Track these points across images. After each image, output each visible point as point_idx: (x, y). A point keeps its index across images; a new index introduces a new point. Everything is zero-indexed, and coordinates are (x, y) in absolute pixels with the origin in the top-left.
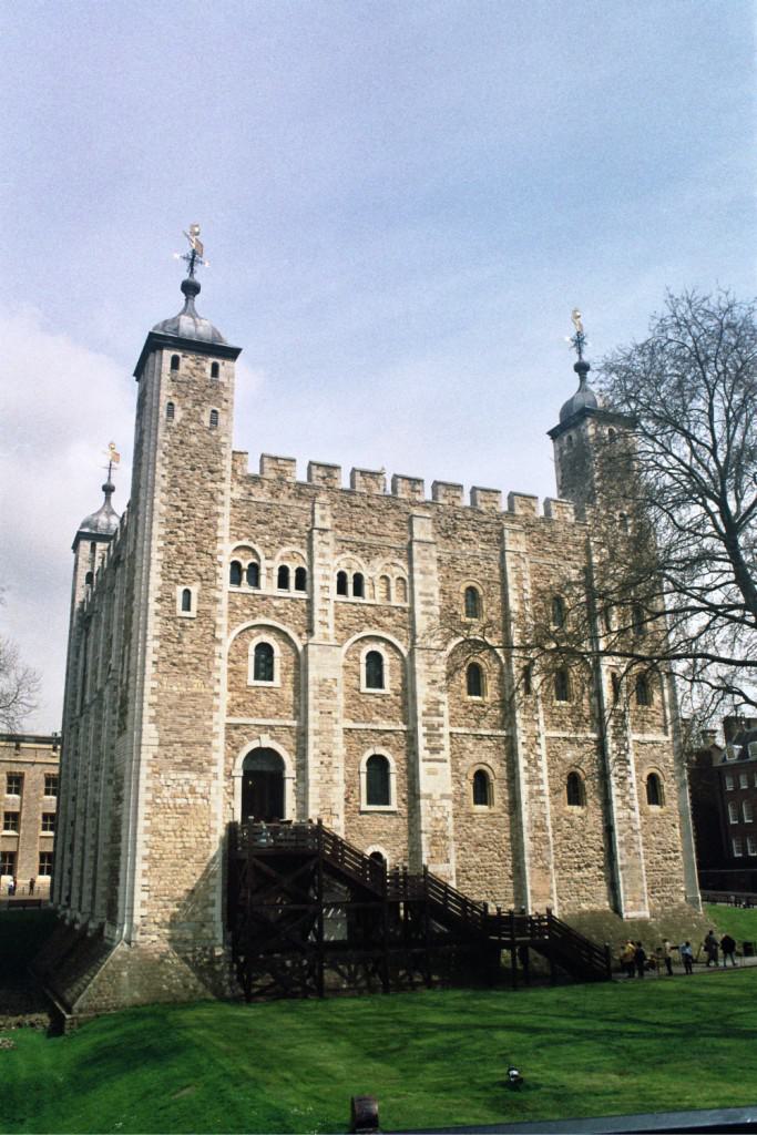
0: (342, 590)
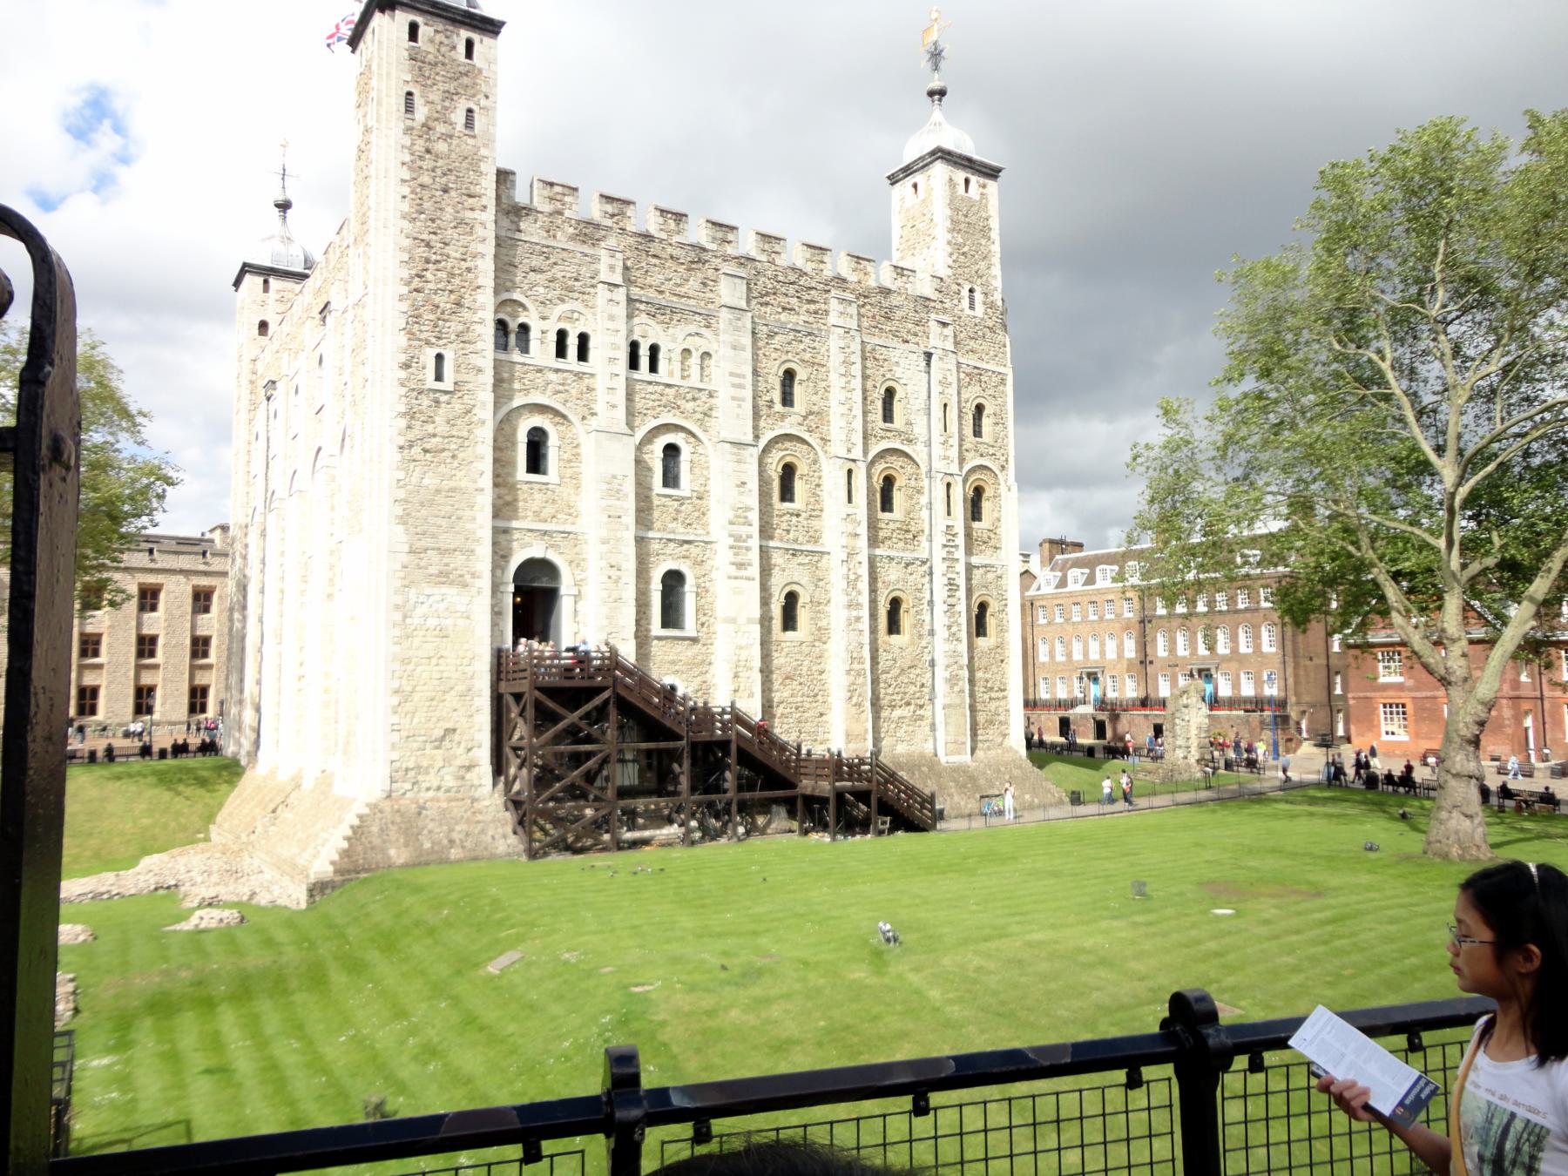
0: (634, 363)
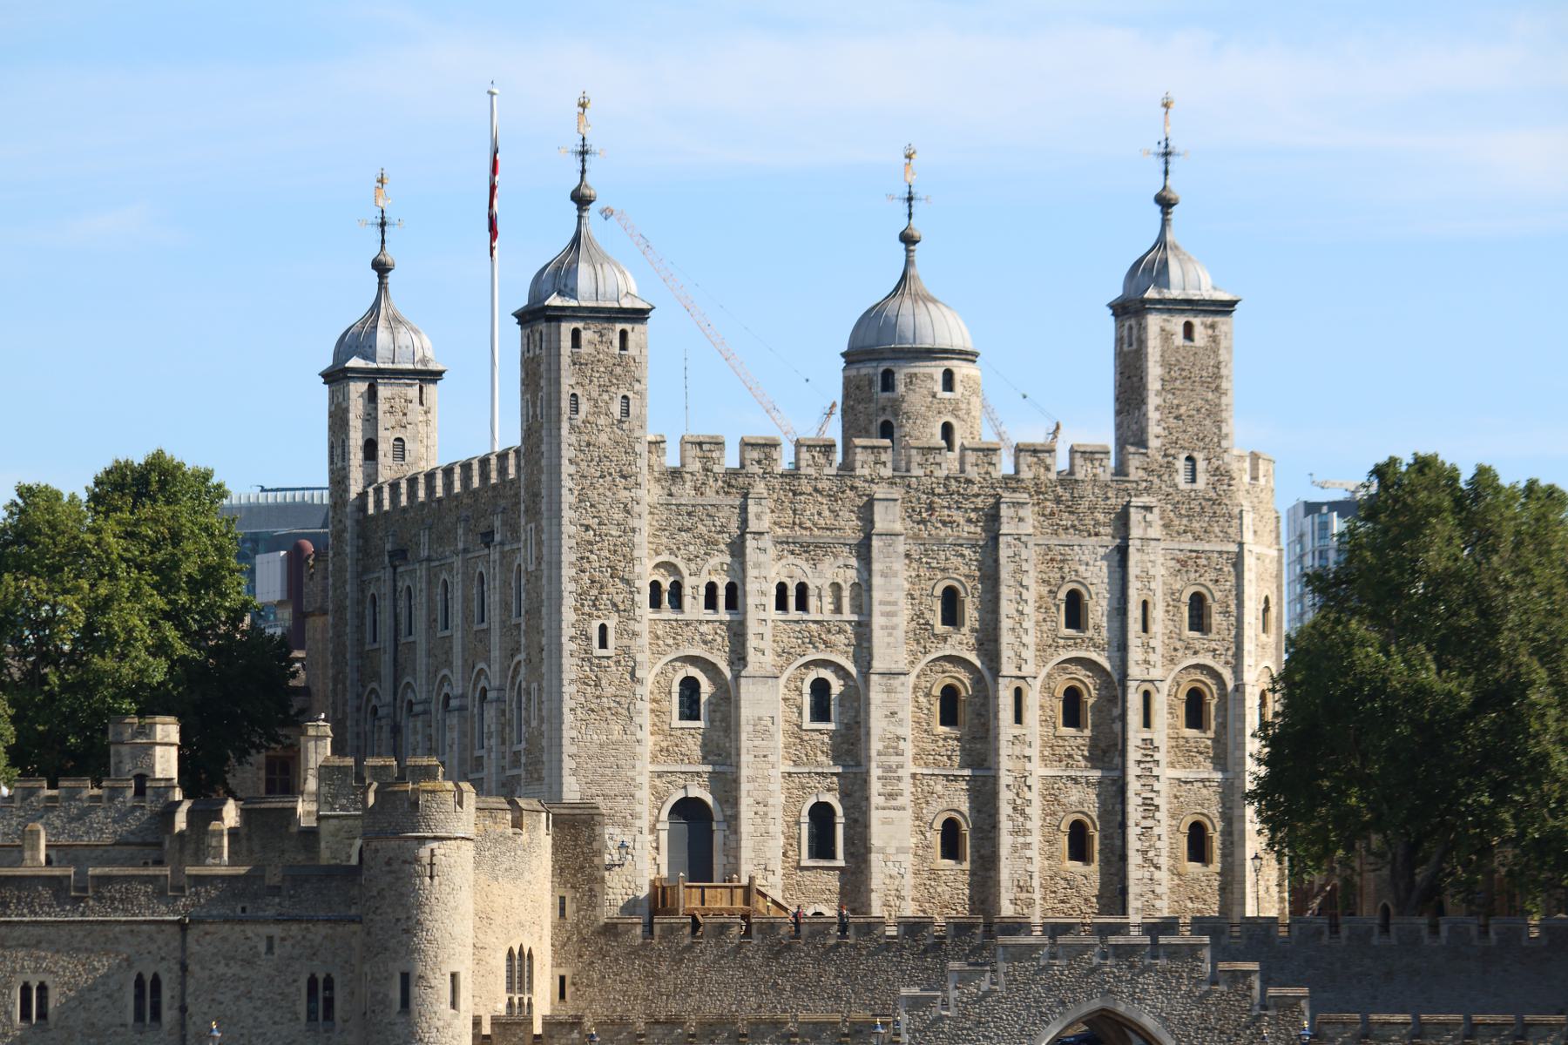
0: (781, 604)
